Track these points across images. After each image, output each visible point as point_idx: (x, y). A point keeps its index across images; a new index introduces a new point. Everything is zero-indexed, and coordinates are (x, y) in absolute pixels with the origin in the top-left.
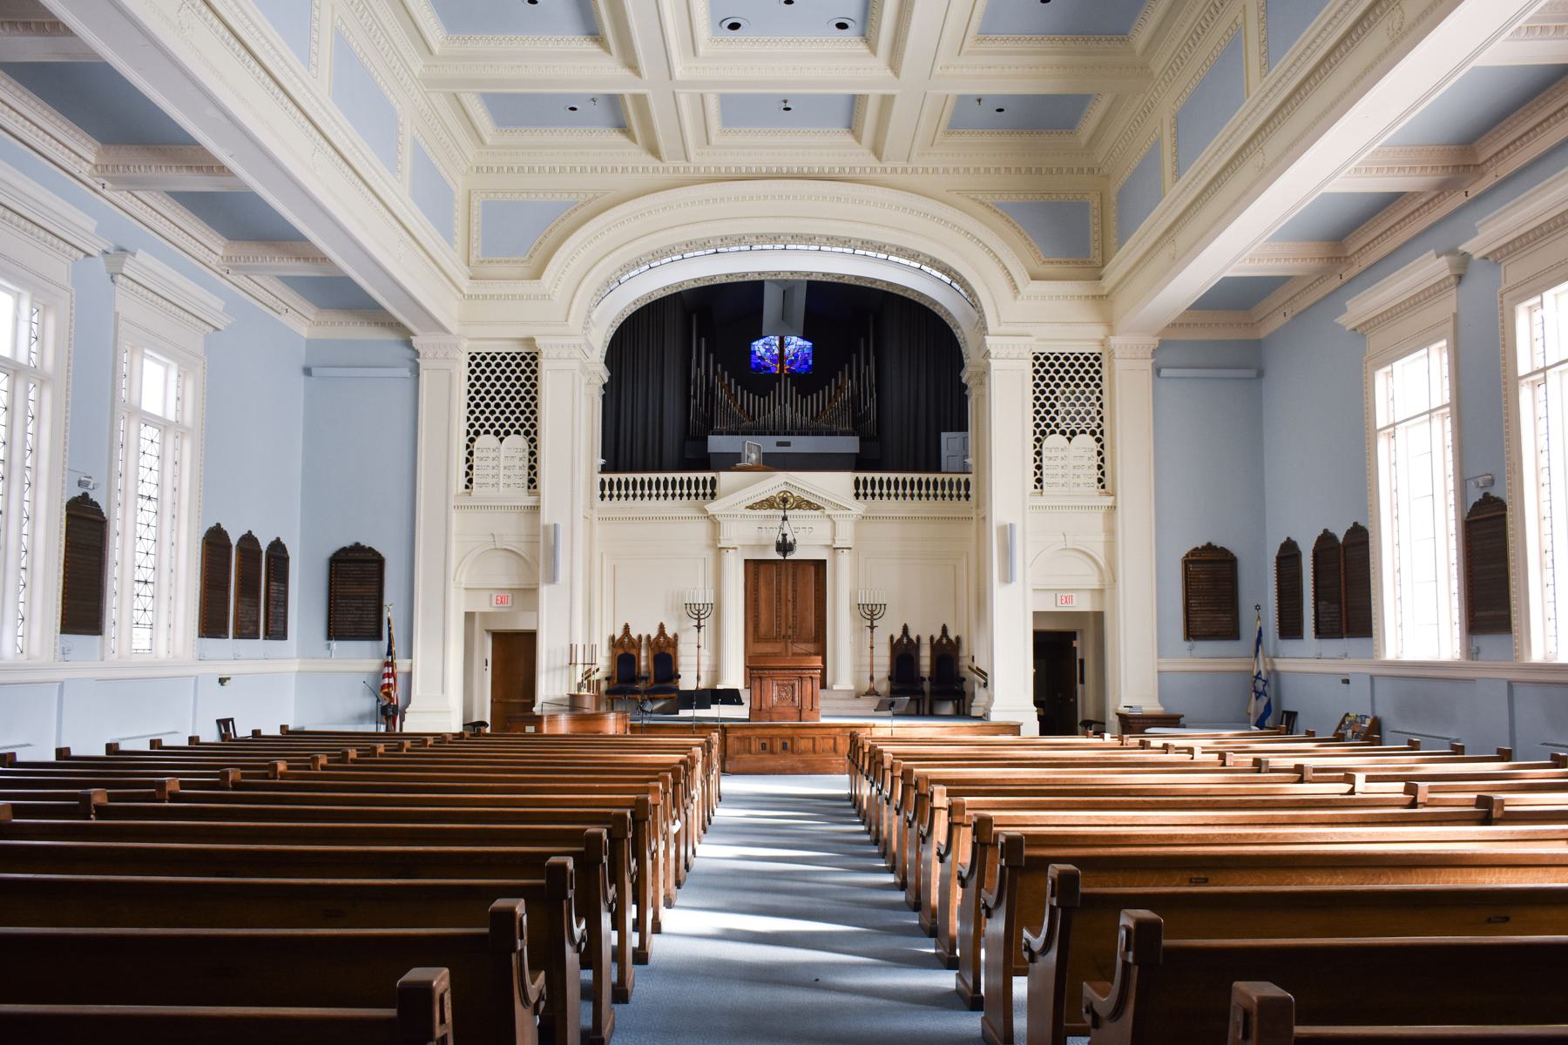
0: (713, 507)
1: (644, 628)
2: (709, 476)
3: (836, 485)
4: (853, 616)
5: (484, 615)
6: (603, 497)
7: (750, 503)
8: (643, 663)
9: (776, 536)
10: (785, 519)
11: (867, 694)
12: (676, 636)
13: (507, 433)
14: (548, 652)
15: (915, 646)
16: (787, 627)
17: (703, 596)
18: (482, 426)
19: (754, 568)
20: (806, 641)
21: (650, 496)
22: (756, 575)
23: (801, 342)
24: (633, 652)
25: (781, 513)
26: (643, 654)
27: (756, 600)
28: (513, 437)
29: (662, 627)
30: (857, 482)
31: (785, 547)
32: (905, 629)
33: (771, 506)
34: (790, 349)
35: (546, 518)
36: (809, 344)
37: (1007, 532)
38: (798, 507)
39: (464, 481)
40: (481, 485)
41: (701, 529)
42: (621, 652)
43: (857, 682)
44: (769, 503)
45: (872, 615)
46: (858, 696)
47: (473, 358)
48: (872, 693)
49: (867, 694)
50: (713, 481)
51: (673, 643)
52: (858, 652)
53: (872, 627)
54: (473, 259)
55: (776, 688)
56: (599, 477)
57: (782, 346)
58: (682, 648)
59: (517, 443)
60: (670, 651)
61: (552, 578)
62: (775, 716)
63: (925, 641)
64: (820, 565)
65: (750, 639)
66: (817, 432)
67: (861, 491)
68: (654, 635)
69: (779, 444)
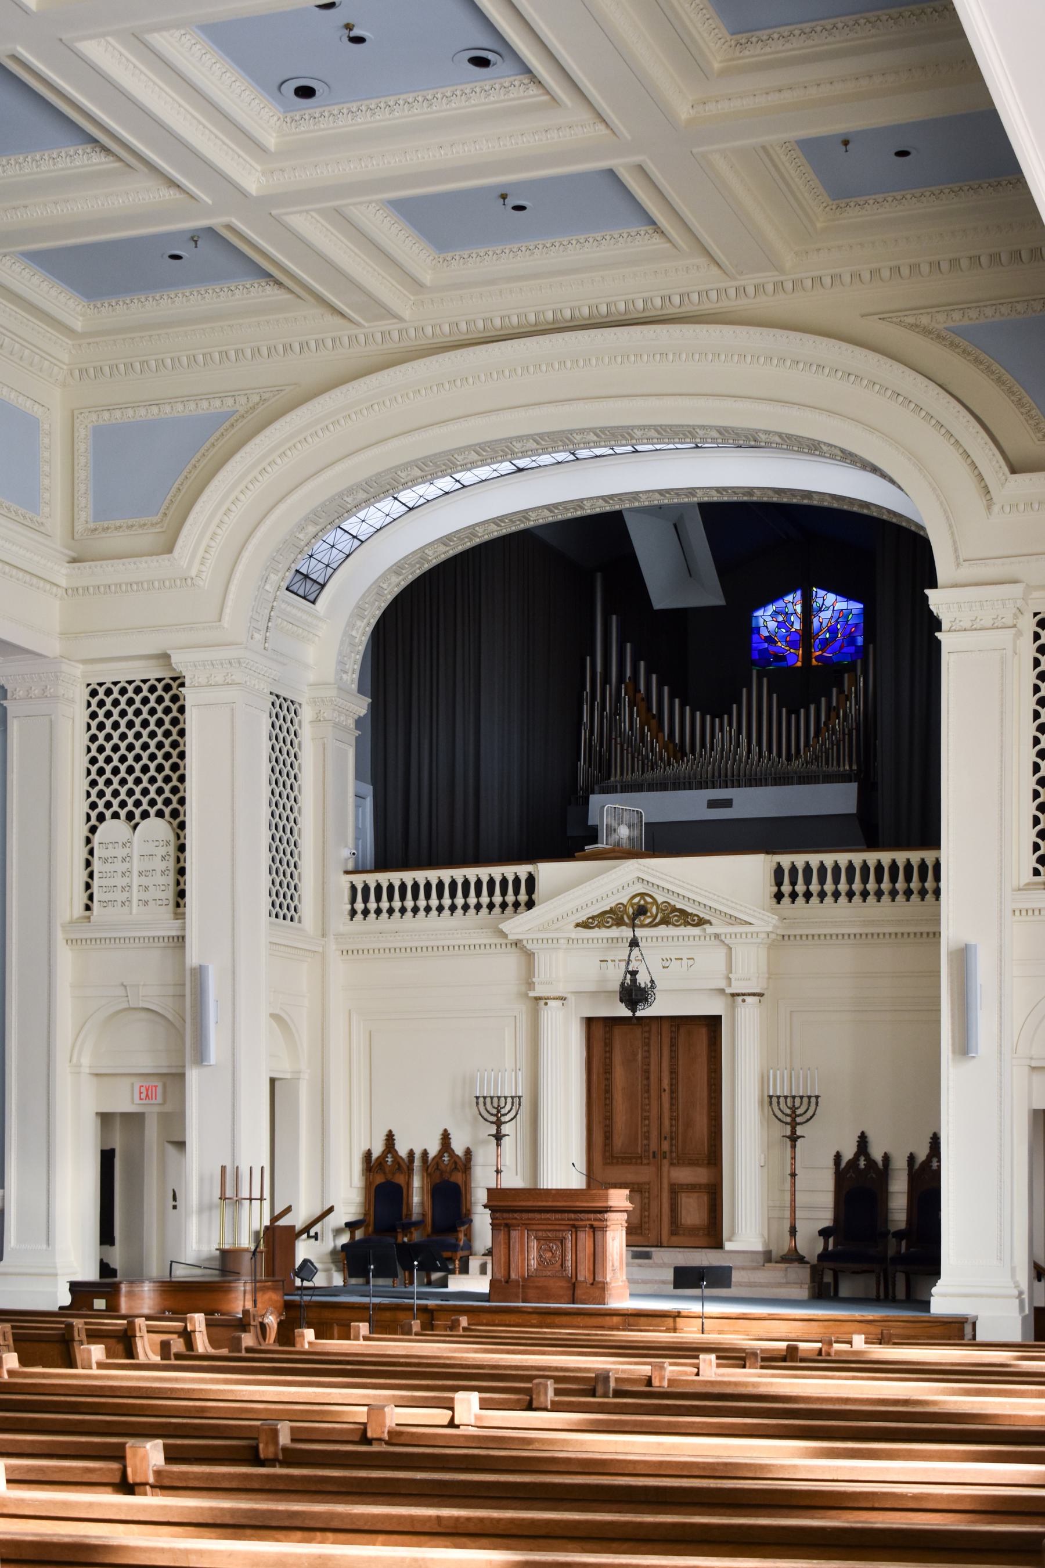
0: (519, 925)
1: (418, 1139)
2: (522, 870)
3: (732, 882)
5: (125, 1115)
6: (353, 913)
7: (582, 917)
8: (416, 1199)
9: (615, 976)
10: (634, 943)
12: (468, 1152)
13: (145, 815)
14: (201, 1180)
15: (882, 1172)
16: (661, 1137)
17: (510, 1083)
18: (108, 805)
19: (599, 1032)
20: (693, 1163)
21: (453, 908)
22: (608, 1045)
23: (842, 605)
24: (400, 1179)
25: (627, 933)
26: (416, 1182)
27: (608, 1091)
28: (153, 821)
29: (446, 1137)
30: (779, 871)
31: (633, 993)
32: (863, 1141)
33: (619, 923)
34: (823, 619)
35: (194, 956)
36: (856, 606)
37: (963, 956)
38: (665, 922)
39: (82, 898)
40: (105, 903)
41: (506, 966)
42: (379, 1179)
44: (613, 917)
45: (794, 1115)
47: (94, 693)
48: (793, 1257)
50: (531, 880)
51: (465, 1164)
53: (794, 1138)
54: (79, 528)
55: (534, 1244)
56: (345, 881)
57: (808, 612)
59: (157, 829)
60: (458, 1178)
61: (200, 1057)
62: (531, 1293)
63: (900, 1164)
64: (713, 1023)
65: (598, 1157)
66: (781, 779)
67: (786, 888)
68: (433, 1150)
69: (713, 804)
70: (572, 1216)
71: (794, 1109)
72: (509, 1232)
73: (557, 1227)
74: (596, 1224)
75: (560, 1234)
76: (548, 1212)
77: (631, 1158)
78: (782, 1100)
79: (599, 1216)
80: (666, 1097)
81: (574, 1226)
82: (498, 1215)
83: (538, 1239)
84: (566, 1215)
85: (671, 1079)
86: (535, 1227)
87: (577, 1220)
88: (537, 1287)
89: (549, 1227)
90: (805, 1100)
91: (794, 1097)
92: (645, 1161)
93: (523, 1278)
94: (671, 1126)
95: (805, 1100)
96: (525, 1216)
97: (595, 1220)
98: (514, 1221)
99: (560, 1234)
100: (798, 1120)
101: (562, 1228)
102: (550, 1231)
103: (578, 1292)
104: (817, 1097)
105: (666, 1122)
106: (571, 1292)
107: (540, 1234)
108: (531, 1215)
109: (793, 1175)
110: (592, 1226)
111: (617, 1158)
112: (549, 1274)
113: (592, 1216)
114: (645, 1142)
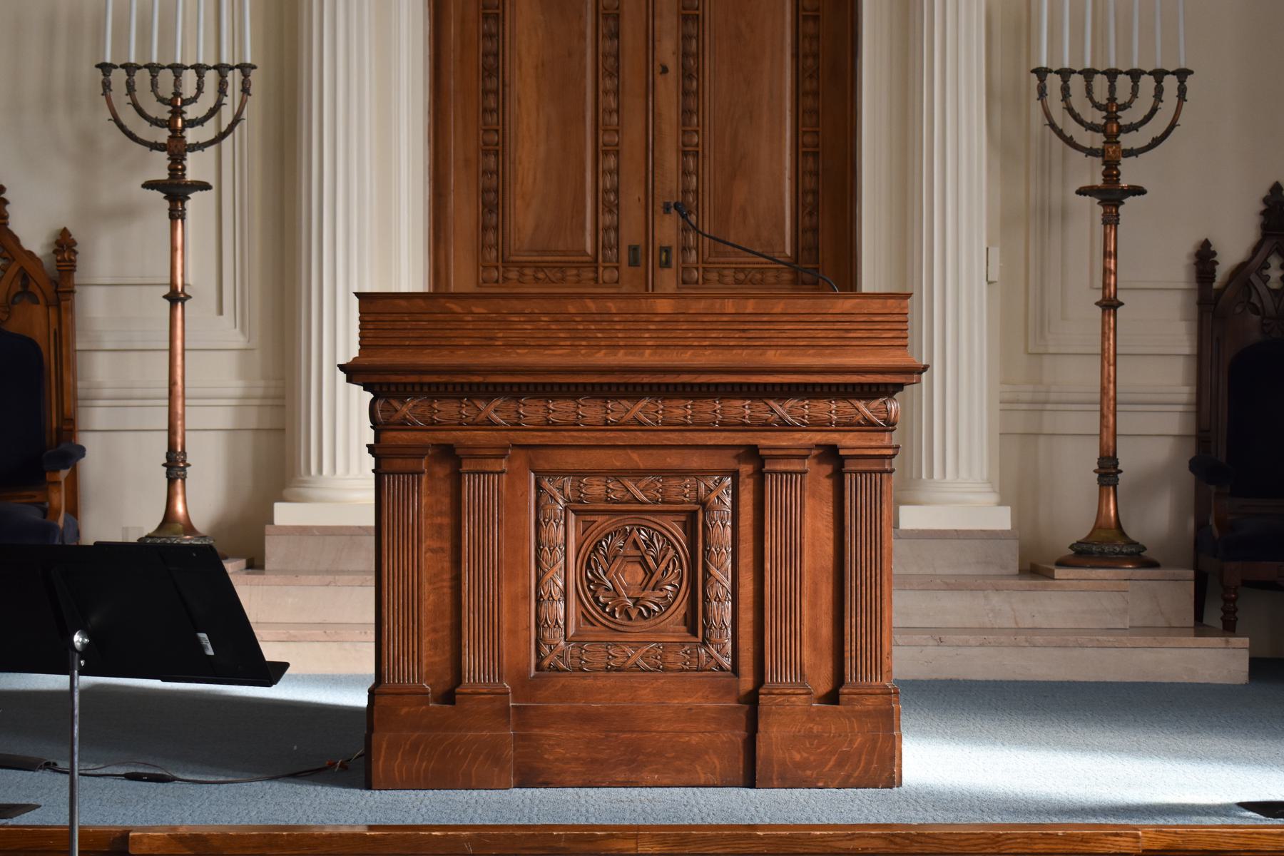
4: (1003, 148)
11: (1086, 554)
43: (1020, 487)
45: (1112, 128)
46: (1034, 569)
49: (1086, 554)
52: (1025, 330)
53: (1111, 195)
55: (566, 534)
58: (98, 309)
70: (743, 409)
71: (1112, 109)
72: (457, 478)
73: (673, 460)
74: (848, 441)
75: (683, 490)
76: (633, 392)
77: (561, 267)
78: (1077, 82)
79: (865, 409)
80: (668, 90)
81: (752, 453)
82: (406, 409)
83: (578, 507)
84: (713, 408)
85: (686, 38)
86: (571, 460)
87: (765, 426)
88: (586, 718)
89: (638, 460)
90: (1147, 83)
91: (1112, 74)
92: (606, 275)
93: (524, 685)
94: (686, 173)
95: (1147, 83)
96: (532, 410)
97: (847, 425)
98: (481, 436)
99: (683, 490)
100: (1127, 141)
101: (696, 461)
102: (638, 474)
103: (772, 734)
104: (1182, 74)
105: (671, 160)
106: (740, 734)
107: (596, 488)
108: (561, 409)
109: (1110, 305)
110: (830, 454)
111: (521, 266)
112: (636, 657)
113: (831, 409)
114: (606, 219)
